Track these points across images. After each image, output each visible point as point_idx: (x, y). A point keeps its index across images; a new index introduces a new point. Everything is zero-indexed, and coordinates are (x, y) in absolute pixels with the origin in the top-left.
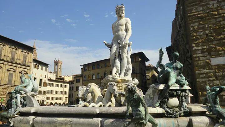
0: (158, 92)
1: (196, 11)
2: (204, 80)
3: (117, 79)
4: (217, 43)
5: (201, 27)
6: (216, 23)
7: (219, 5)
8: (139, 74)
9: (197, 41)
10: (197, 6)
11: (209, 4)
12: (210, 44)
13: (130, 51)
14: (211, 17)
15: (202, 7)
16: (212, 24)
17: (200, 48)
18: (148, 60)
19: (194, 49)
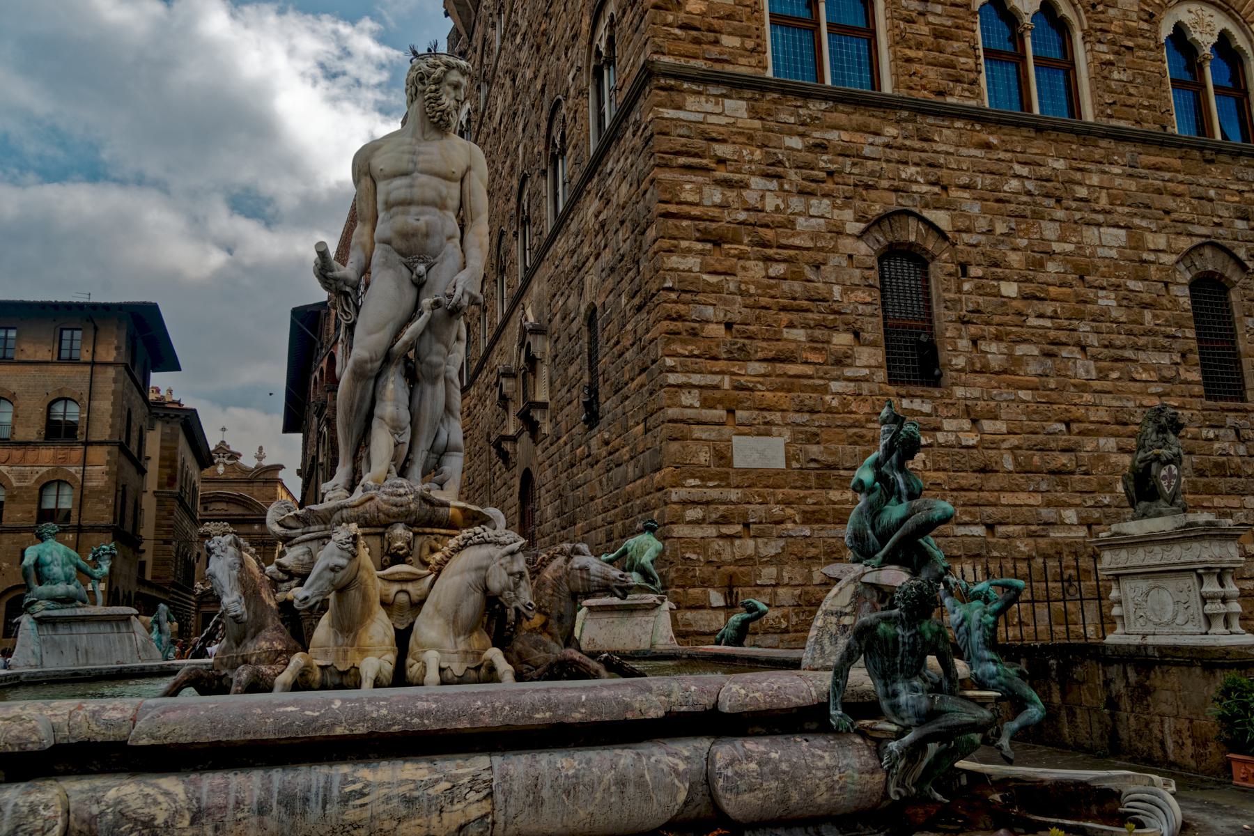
0: (875, 599)
1: (696, 198)
2: (698, 532)
3: (447, 505)
4: (763, 372)
5: (708, 284)
6: (766, 281)
7: (782, 207)
8: (106, 449)
9: (690, 348)
10: (700, 179)
11: (746, 186)
12: (735, 370)
13: (458, 339)
14: (749, 249)
15: (719, 189)
16: (753, 283)
17: (696, 379)
18: (172, 365)
19: (672, 379)
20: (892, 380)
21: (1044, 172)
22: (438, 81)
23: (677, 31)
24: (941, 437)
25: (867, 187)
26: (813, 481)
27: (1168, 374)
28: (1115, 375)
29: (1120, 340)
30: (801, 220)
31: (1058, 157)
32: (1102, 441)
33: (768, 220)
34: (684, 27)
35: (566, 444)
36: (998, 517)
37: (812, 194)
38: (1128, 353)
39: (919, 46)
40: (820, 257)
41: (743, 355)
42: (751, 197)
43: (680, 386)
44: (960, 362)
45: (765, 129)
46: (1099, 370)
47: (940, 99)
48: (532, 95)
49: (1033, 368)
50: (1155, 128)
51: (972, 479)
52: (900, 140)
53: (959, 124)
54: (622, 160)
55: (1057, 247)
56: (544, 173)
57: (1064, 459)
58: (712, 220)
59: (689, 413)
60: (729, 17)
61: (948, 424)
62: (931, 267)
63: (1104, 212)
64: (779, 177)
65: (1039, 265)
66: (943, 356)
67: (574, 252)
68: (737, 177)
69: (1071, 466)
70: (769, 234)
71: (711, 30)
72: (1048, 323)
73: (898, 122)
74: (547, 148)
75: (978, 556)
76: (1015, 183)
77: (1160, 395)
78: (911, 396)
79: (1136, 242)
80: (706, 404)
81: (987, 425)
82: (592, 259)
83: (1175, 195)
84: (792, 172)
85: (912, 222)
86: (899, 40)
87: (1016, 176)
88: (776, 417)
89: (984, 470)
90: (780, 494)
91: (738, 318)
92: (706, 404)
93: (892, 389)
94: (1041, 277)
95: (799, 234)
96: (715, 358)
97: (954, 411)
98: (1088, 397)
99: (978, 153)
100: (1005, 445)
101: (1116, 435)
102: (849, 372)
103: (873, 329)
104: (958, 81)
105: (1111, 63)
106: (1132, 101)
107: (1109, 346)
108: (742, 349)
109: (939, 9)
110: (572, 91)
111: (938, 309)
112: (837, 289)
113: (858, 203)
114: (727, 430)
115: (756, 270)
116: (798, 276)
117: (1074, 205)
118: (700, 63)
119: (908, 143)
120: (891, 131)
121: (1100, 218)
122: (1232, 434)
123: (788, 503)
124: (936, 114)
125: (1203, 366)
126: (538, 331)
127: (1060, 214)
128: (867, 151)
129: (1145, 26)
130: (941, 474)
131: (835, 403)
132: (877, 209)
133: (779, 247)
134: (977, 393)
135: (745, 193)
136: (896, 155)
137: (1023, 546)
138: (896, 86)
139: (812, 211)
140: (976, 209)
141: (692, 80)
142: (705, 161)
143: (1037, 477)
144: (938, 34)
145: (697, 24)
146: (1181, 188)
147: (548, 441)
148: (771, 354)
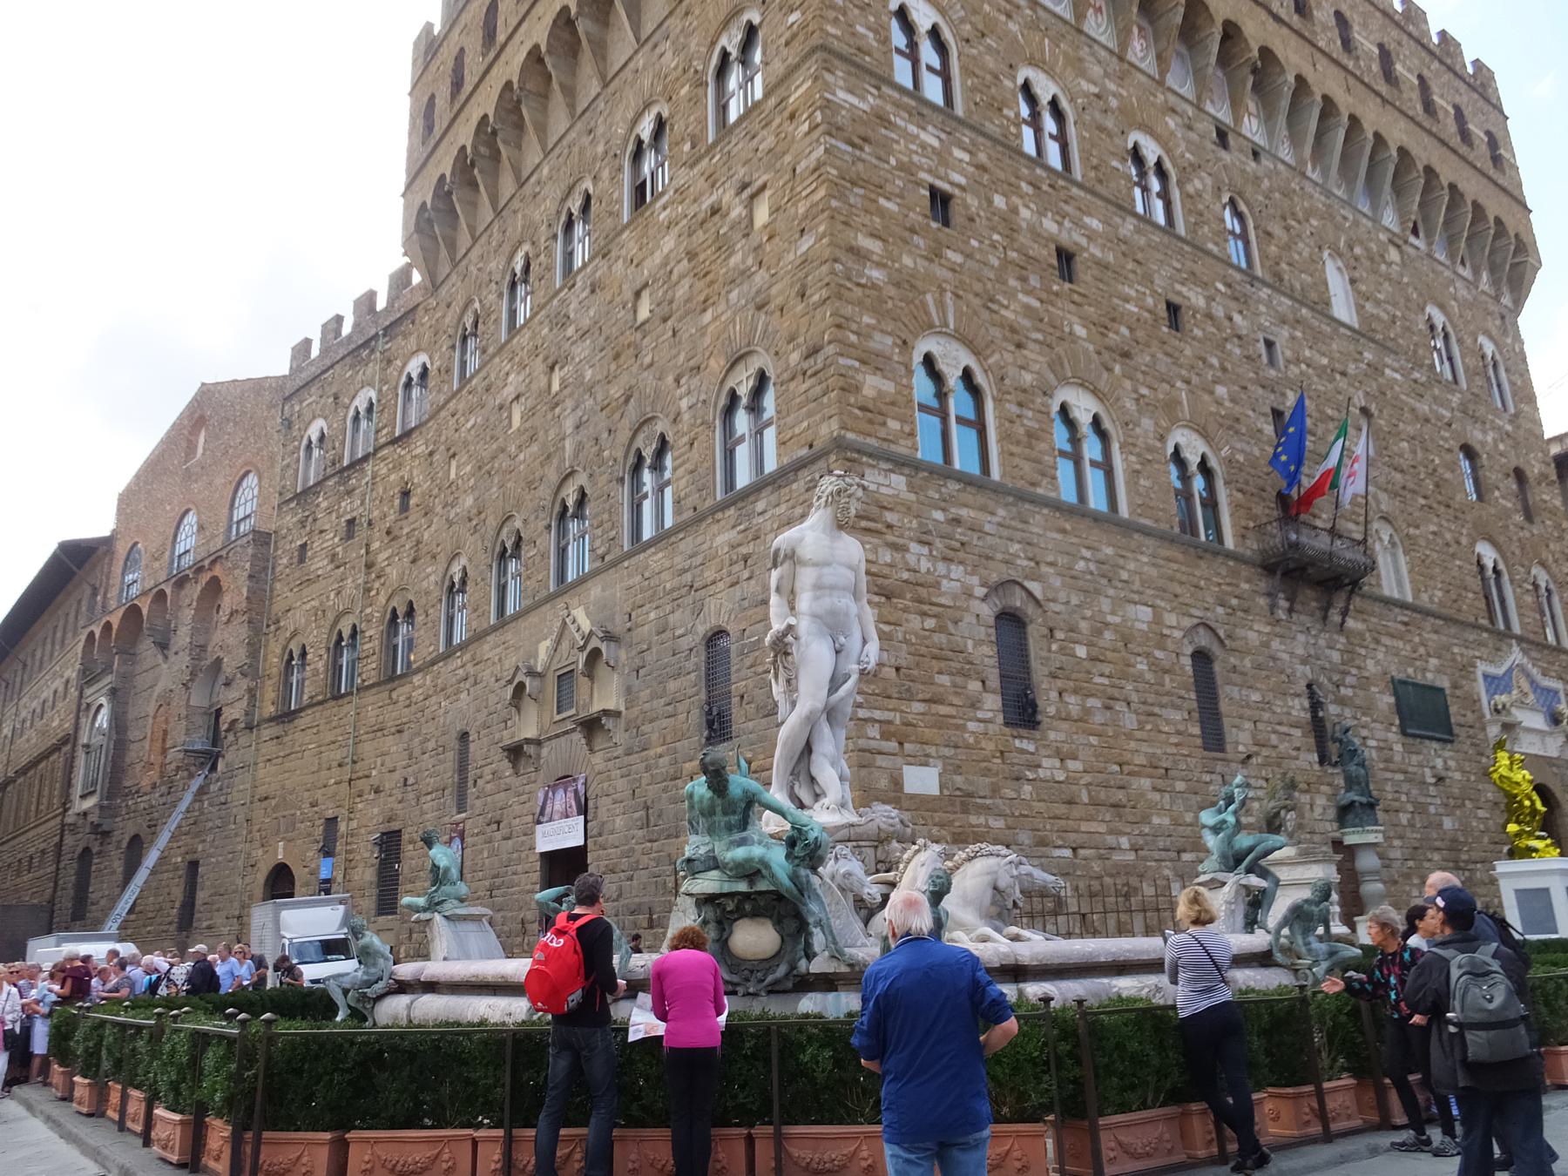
10: (875, 541)
17: (877, 714)
19: (862, 713)
20: (1007, 724)
21: (1100, 556)
22: (850, 496)
23: (857, 411)
24: (1042, 773)
25: (988, 558)
26: (958, 808)
27: (1182, 728)
28: (1149, 727)
29: (1151, 698)
30: (945, 582)
31: (1109, 545)
32: (1143, 781)
33: (921, 580)
34: (863, 409)
35: (661, 756)
36: (1079, 842)
37: (951, 560)
38: (1156, 710)
39: (1018, 443)
40: (958, 614)
41: (910, 697)
42: (911, 559)
43: (865, 720)
44: (1052, 710)
45: (919, 502)
46: (1139, 722)
47: (1032, 489)
48: (600, 397)
49: (1099, 718)
50: (1164, 526)
51: (1061, 809)
52: (1008, 522)
53: (1045, 511)
54: (783, 507)
55: (1110, 618)
56: (622, 479)
57: (1120, 796)
58: (885, 577)
59: (873, 744)
60: (893, 404)
61: (1046, 763)
62: (1031, 629)
63: (1138, 592)
64: (929, 544)
65: (1098, 632)
66: (1040, 703)
67: (685, 571)
68: (900, 541)
69: (1124, 800)
70: (923, 592)
71: (881, 413)
72: (1106, 681)
73: (1006, 505)
74: (626, 457)
75: (1067, 874)
76: (1081, 565)
77: (1176, 745)
78: (1020, 737)
79: (1157, 620)
80: (885, 736)
81: (1071, 764)
82: (721, 585)
83: (1182, 583)
84: (938, 540)
85: (1017, 589)
86: (1005, 437)
87: (1083, 558)
88: (932, 750)
89: (1070, 802)
90: (938, 816)
91: (904, 663)
92: (885, 736)
93: (1007, 730)
94: (1101, 643)
95: (944, 594)
96: (889, 697)
97: (1049, 752)
98: (1133, 744)
99: (1059, 536)
100: (1082, 782)
101: (1151, 777)
102: (980, 715)
103: (994, 681)
104: (1043, 475)
105: (1138, 472)
106: (1152, 504)
107: (1144, 703)
108: (908, 690)
109: (1030, 414)
110: (686, 417)
111: (1035, 664)
112: (970, 643)
113: (983, 571)
114: (899, 760)
115: (915, 622)
116: (941, 629)
117: (1120, 585)
118: (872, 441)
119: (1013, 523)
120: (1001, 512)
121: (1136, 597)
122: (1219, 778)
123: (942, 825)
124: (1032, 502)
125: (1202, 722)
126: (609, 637)
127: (1111, 592)
128: (987, 528)
129: (1158, 444)
130: (1042, 804)
131: (971, 740)
132: (994, 578)
133: (932, 604)
134: (1062, 737)
135: (908, 556)
136: (1005, 533)
137: (1096, 867)
138: (1003, 475)
139: (953, 576)
140: (1057, 582)
141: (870, 455)
142: (879, 526)
143: (1102, 809)
144: (1031, 435)
145: (871, 406)
146: (1184, 578)
147: (620, 751)
148: (928, 696)
